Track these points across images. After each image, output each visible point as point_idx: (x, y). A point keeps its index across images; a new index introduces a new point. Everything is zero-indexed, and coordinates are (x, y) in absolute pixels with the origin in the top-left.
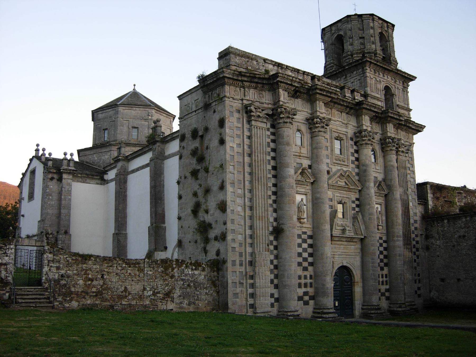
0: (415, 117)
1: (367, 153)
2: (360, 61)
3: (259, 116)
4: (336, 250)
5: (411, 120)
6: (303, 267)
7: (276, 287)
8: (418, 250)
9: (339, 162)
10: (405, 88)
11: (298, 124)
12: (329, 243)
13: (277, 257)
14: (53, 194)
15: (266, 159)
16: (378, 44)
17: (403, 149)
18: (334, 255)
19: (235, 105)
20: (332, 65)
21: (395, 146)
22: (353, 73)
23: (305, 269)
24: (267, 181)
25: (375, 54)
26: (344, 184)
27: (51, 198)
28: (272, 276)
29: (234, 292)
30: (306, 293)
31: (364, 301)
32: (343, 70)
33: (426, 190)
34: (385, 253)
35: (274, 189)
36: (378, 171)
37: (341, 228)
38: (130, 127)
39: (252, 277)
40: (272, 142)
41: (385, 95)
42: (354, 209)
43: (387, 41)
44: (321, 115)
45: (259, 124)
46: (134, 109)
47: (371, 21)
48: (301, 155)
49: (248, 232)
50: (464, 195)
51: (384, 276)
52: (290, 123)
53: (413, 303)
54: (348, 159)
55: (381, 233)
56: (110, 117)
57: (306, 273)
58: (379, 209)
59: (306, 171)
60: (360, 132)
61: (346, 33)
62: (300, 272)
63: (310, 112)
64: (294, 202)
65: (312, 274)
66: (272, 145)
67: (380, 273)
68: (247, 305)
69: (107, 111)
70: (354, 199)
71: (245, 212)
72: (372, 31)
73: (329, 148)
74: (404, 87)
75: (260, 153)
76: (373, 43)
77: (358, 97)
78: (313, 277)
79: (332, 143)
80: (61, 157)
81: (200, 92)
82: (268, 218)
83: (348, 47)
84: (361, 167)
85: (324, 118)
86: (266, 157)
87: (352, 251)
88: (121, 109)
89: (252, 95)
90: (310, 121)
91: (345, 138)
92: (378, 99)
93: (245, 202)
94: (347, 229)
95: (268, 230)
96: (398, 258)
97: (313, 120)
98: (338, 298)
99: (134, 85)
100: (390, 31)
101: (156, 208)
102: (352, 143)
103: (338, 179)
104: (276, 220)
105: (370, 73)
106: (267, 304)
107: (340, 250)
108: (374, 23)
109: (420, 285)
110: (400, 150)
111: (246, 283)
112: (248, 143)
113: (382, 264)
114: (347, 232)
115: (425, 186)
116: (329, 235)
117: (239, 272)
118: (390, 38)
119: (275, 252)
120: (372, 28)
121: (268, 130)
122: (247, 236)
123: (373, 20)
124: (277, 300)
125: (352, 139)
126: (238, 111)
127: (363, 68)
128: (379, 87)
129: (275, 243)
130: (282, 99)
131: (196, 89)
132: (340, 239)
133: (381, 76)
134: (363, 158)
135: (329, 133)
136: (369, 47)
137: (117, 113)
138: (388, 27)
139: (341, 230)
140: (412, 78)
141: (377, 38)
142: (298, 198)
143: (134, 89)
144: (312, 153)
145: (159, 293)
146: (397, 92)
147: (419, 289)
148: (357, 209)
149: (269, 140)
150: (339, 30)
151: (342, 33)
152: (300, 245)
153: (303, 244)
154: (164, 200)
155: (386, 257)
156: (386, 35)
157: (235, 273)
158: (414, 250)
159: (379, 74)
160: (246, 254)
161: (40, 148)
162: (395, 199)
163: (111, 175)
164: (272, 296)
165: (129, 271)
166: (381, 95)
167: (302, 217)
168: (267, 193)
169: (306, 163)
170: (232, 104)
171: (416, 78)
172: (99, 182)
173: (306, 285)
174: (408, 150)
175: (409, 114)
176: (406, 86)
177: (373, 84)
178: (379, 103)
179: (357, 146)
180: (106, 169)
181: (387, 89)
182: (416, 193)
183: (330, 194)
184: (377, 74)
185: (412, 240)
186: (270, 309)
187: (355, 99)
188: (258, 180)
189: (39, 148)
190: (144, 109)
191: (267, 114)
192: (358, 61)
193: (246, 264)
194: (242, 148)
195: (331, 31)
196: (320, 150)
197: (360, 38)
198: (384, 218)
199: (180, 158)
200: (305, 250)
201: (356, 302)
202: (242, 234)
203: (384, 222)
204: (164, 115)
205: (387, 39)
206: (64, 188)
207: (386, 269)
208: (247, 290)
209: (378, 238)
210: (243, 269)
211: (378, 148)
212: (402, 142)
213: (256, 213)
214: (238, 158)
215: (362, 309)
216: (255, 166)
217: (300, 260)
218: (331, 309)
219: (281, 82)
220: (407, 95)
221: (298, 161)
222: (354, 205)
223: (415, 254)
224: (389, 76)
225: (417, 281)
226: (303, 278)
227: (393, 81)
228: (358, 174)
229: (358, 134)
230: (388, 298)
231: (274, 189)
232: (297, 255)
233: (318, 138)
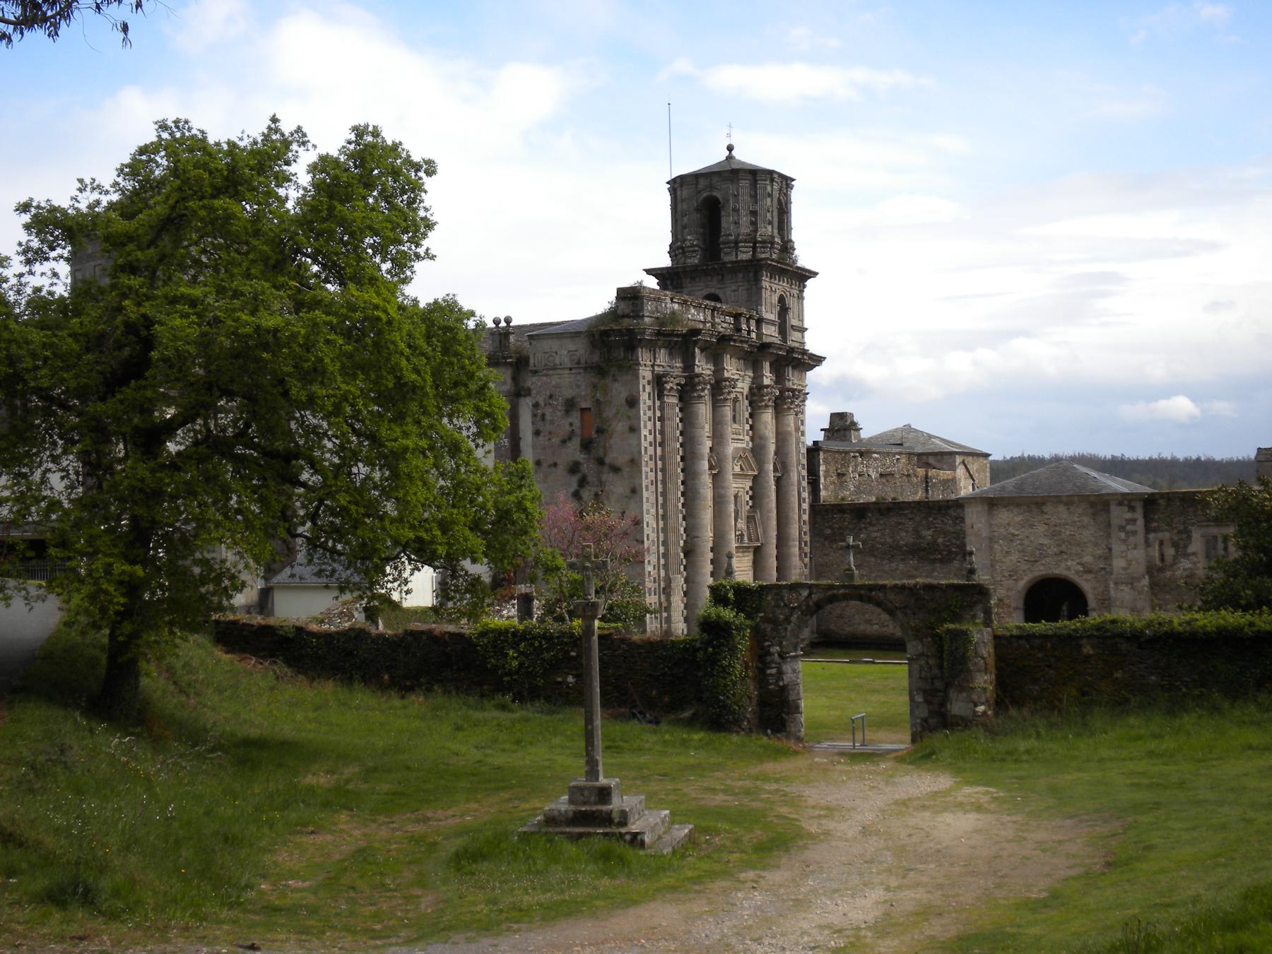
25: (773, 243)
47: (768, 182)
61: (728, 201)
70: (748, 489)
72: (769, 200)
76: (770, 223)
83: (726, 222)
84: (757, 441)
108: (772, 186)
120: (770, 195)
141: (775, 214)
149: (678, 420)
150: (712, 187)
175: (803, 337)
181: (782, 300)
191: (678, 384)
214: (651, 451)
228: (752, 450)
229: (756, 391)
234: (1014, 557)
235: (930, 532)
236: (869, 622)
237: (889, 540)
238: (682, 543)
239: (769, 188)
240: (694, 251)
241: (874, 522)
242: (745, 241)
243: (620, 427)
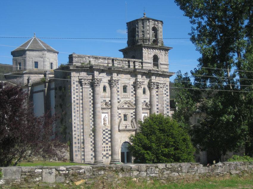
1: (140, 91)
9: (125, 97)
11: (104, 83)
20: (130, 43)
30: (107, 154)
37: (125, 126)
39: (84, 148)
45: (86, 86)
48: (106, 96)
49: (82, 130)
57: (107, 145)
65: (110, 145)
72: (148, 28)
74: (165, 53)
85: (116, 80)
89: (83, 74)
91: (128, 85)
106: (90, 158)
114: (127, 127)
123: (149, 22)
132: (124, 130)
136: (146, 36)
138: (158, 23)
146: (161, 57)
153: (106, 134)
156: (157, 27)
159: (151, 50)
164: (92, 155)
177: (147, 55)
182: (169, 106)
194: (79, 97)
200: (107, 136)
210: (79, 145)
226: (106, 147)
238: (91, 129)
239: (148, 24)
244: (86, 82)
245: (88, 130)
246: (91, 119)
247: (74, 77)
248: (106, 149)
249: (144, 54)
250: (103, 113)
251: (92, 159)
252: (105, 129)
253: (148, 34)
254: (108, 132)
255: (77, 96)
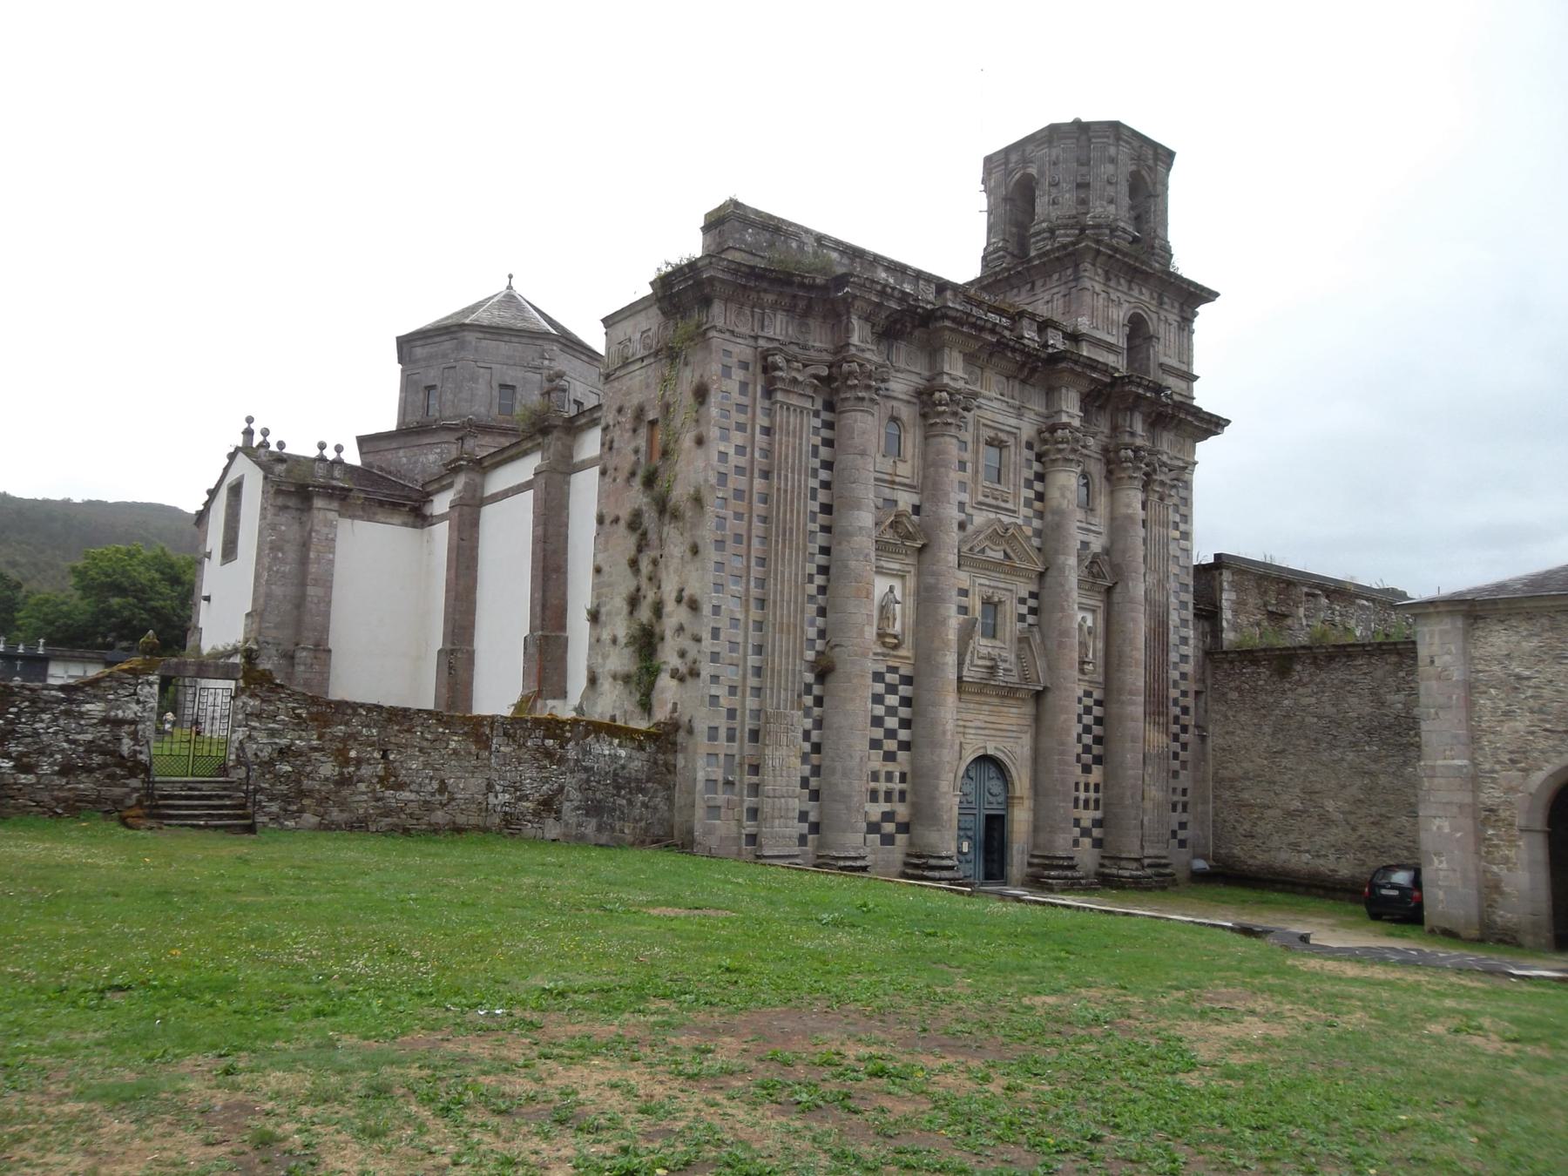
0: (1205, 397)
1: (1066, 482)
2: (1071, 249)
3: (795, 381)
4: (969, 717)
5: (1195, 403)
6: (885, 752)
7: (815, 795)
8: (1185, 729)
9: (993, 502)
10: (1186, 321)
11: (895, 403)
12: (951, 698)
13: (819, 724)
14: (287, 547)
15: (806, 486)
16: (1125, 201)
17: (1162, 477)
18: (965, 727)
19: (735, 349)
21: (1141, 468)
22: (1050, 276)
23: (890, 757)
24: (804, 540)
26: (1000, 555)
27: (280, 555)
28: (807, 769)
29: (712, 804)
30: (888, 817)
31: (1036, 846)
32: (1028, 269)
33: (1217, 583)
34: (1097, 730)
35: (821, 559)
36: (1093, 528)
37: (988, 663)
38: (495, 385)
39: (755, 769)
40: (823, 445)
41: (1130, 338)
42: (1022, 618)
43: (1150, 196)
44: (952, 383)
45: (794, 400)
46: (507, 338)
48: (898, 479)
50: (1324, 601)
51: (1092, 787)
52: (872, 400)
53: (1163, 861)
54: (1016, 496)
55: (1090, 682)
56: (445, 356)
57: (890, 766)
58: (1089, 623)
59: (905, 520)
60: (1053, 429)
62: (876, 762)
63: (926, 374)
64: (869, 595)
66: (824, 452)
67: (1082, 780)
68: (740, 838)
69: (437, 339)
71: (747, 611)
72: (1110, 168)
73: (969, 465)
75: (793, 472)
77: (1056, 341)
78: (909, 777)
79: (977, 452)
80: (313, 453)
81: (654, 311)
82: (802, 629)
84: (1049, 517)
85: (958, 391)
86: (806, 481)
87: (1014, 721)
88: (471, 337)
89: (779, 327)
90: (925, 397)
91: (1011, 441)
92: (1110, 348)
93: (747, 590)
94: (1002, 665)
95: (802, 658)
96: (1128, 745)
97: (931, 394)
98: (970, 833)
99: (510, 277)
100: (1161, 168)
101: (544, 592)
102: (1031, 455)
103: (987, 543)
104: (822, 634)
105: (1093, 280)
107: (981, 717)
109: (1185, 817)
110: (1155, 477)
111: (741, 781)
112: (765, 446)
113: (1087, 758)
114: (1001, 673)
115: (1217, 573)
116: (953, 676)
117: (726, 755)
118: (1159, 187)
119: (816, 711)
120: (1113, 160)
121: (817, 414)
122: (750, 671)
123: (1118, 138)
124: (815, 828)
125: (1030, 446)
126: (744, 366)
127: (1077, 266)
128: (1115, 317)
129: (817, 690)
130: (855, 339)
131: (647, 303)
133: (1125, 289)
134: (1054, 494)
135: (971, 428)
136: (1100, 210)
137: (462, 346)
138: (1156, 159)
139: (988, 667)
140: (1208, 295)
141: (1124, 189)
142: (881, 586)
143: (510, 287)
144: (925, 477)
145: (525, 798)
146: (1162, 331)
147: (1183, 825)
148: (1031, 619)
149: (817, 440)
151: (1033, 170)
152: (878, 699)
154: (566, 573)
155: (1098, 740)
156: (1148, 180)
157: (713, 759)
158: (1175, 728)
160: (743, 713)
161: (257, 427)
162: (1132, 601)
163: (441, 504)
164: (803, 816)
165: (453, 745)
166: (1118, 338)
167: (890, 631)
168: (804, 568)
169: (906, 500)
170: (730, 347)
171: (1217, 295)
172: (410, 520)
173: (888, 796)
174: (1177, 480)
175: (1190, 389)
176: (1189, 316)
177: (1101, 307)
178: (1110, 359)
179: (1043, 463)
180: (429, 489)
182: (1192, 589)
183: (963, 578)
184: (1112, 284)
185: (1171, 704)
186: (796, 850)
187: (1045, 346)
188: (784, 534)
189: (252, 426)
190: (530, 341)
191: (816, 377)
192: (1064, 247)
193: (742, 737)
195: (1007, 163)
196: (943, 470)
197: (1079, 186)
198: (1100, 645)
199: (603, 473)
200: (891, 711)
201: (1015, 847)
202: (737, 665)
203: (1100, 654)
204: (583, 357)
205: (1151, 188)
206: (317, 532)
207: (1097, 770)
208: (742, 801)
209: (1080, 693)
211: (1097, 469)
212: (1165, 458)
213: (775, 614)
215: (1030, 865)
216: (778, 501)
217: (878, 733)
218: (950, 858)
219: (855, 297)
220: (1190, 339)
221: (887, 493)
222: (1024, 610)
223: (1176, 738)
224: (1144, 290)
225: (1180, 808)
226: (882, 777)
227: (1154, 302)
229: (1047, 435)
230: (1098, 843)
231: (821, 559)
232: (869, 721)
233: (942, 439)
234: (1521, 724)
235: (1401, 697)
236: (1295, 847)
237: (1330, 710)
238: (810, 655)
239: (1112, 150)
240: (999, 258)
241: (1306, 680)
242: (1066, 227)
243: (687, 441)
244: (794, 374)
245: (793, 665)
246: (811, 598)
247: (727, 335)
248: (882, 786)
249: (1087, 297)
250: (880, 571)
251: (802, 840)
252: (884, 669)
253: (1111, 201)
254: (901, 687)
255: (740, 450)
